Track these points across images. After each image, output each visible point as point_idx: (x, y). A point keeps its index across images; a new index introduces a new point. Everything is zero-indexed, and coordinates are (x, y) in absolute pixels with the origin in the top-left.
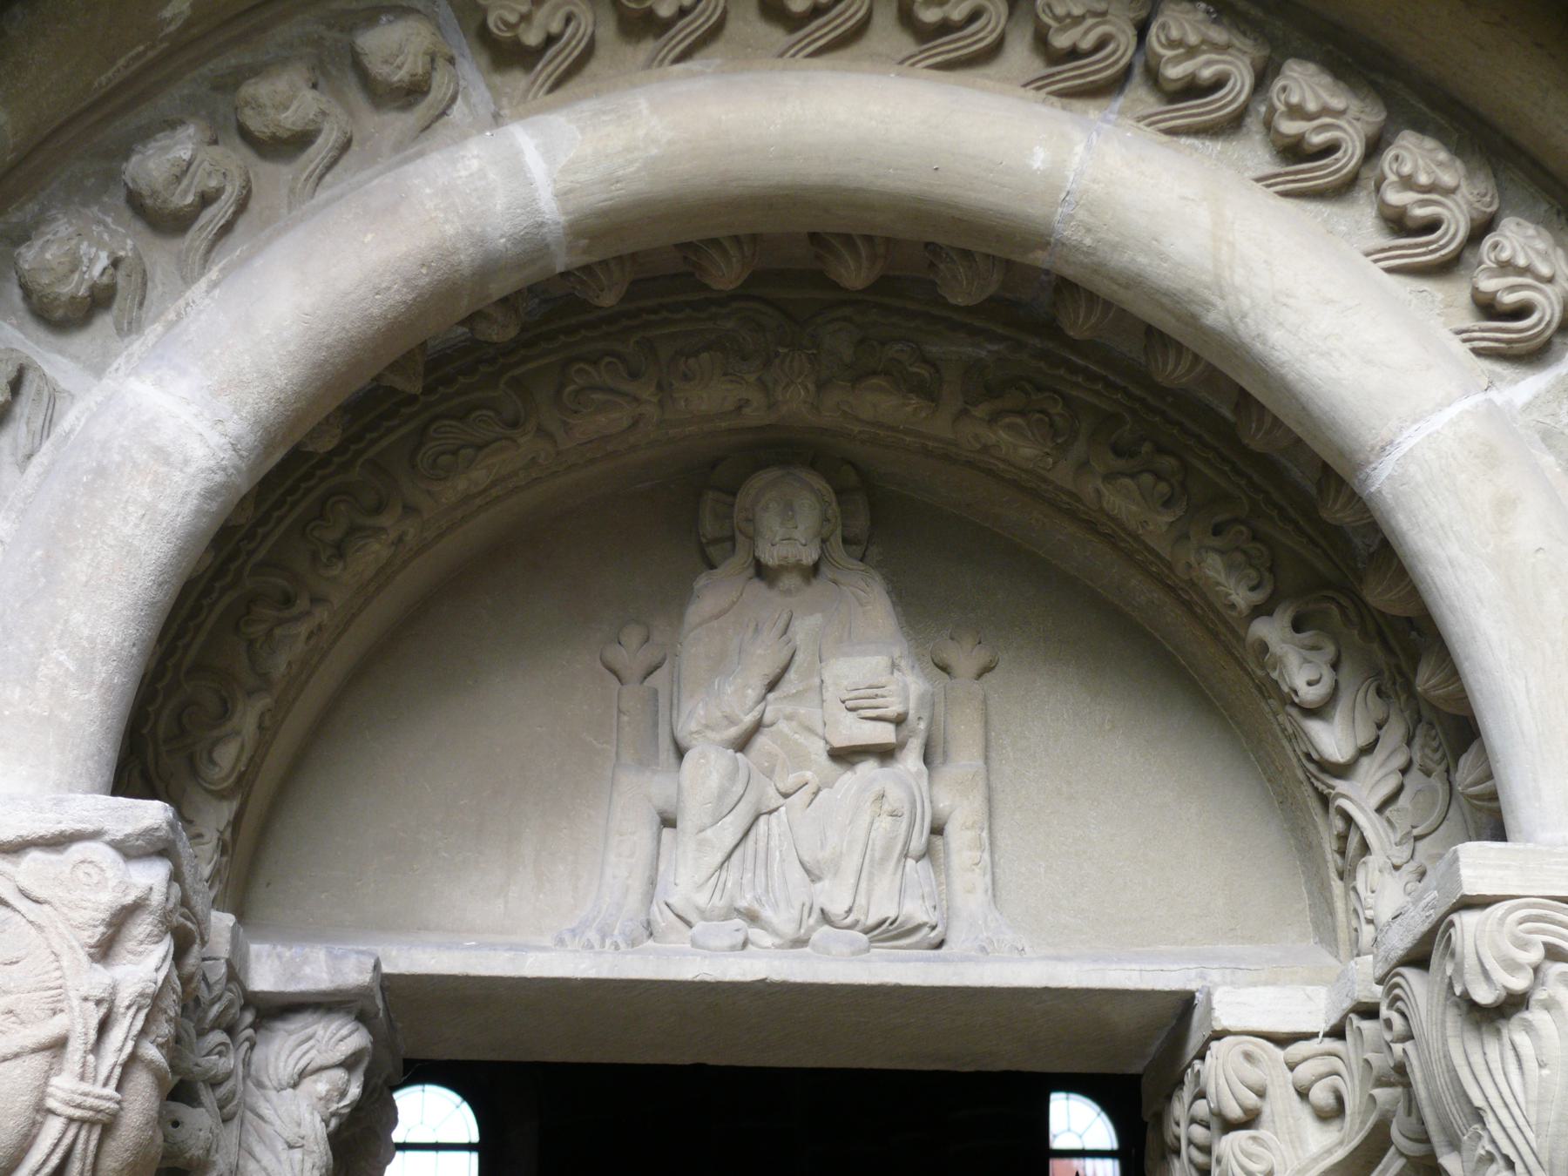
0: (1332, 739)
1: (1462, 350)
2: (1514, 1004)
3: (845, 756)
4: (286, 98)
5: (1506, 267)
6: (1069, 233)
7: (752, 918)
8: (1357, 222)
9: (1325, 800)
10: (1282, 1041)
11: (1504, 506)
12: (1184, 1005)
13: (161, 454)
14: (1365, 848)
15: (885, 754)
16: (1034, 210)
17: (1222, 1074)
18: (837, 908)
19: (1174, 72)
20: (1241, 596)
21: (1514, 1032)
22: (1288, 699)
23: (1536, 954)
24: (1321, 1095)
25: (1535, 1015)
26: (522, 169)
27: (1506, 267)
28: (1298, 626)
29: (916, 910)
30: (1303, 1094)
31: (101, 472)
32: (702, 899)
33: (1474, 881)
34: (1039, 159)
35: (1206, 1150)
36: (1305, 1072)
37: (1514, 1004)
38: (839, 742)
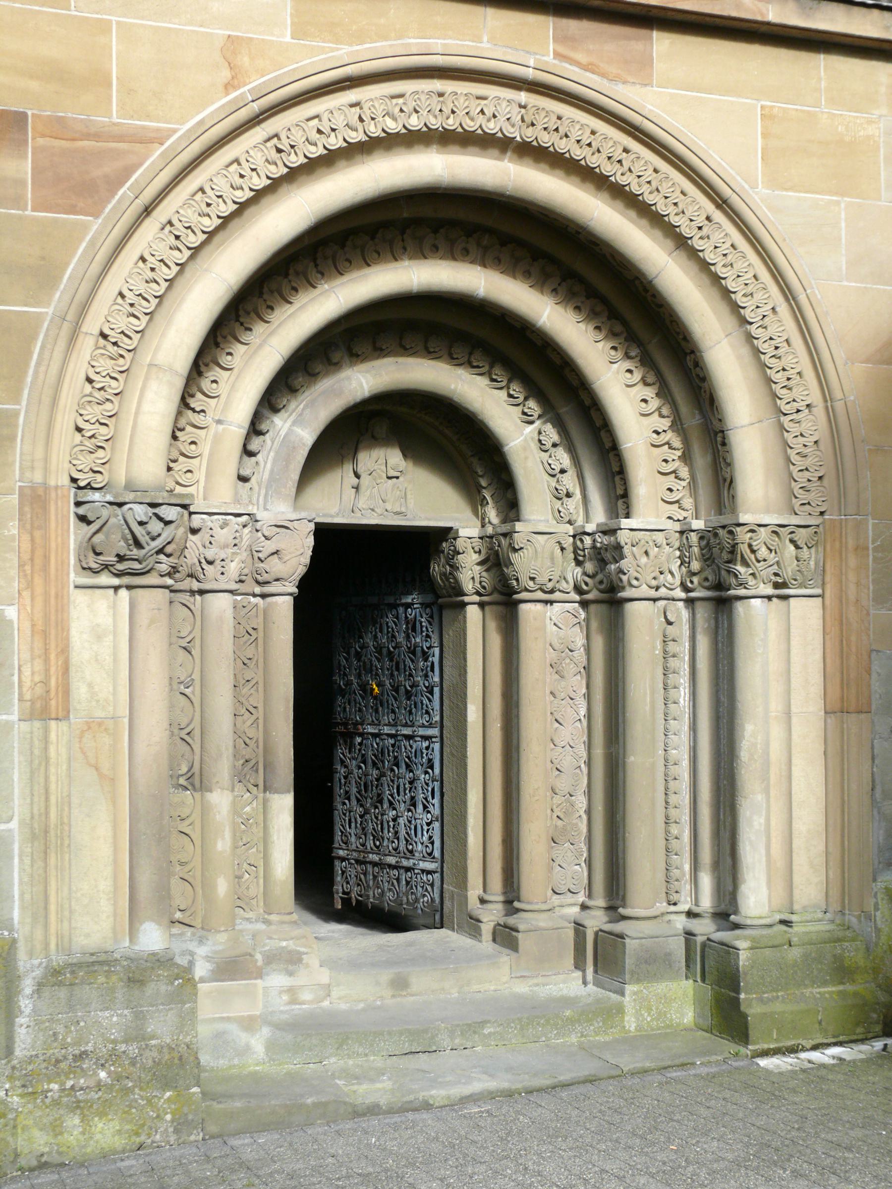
0: (483, 483)
1: (519, 421)
2: (522, 548)
3: (389, 478)
4: (319, 367)
5: (529, 408)
6: (456, 400)
7: (373, 510)
8: (503, 394)
9: (479, 492)
10: (470, 538)
11: (526, 458)
12: (451, 528)
13: (304, 444)
14: (488, 503)
15: (397, 478)
16: (450, 395)
17: (460, 544)
18: (389, 509)
19: (475, 364)
20: (470, 454)
21: (520, 552)
22: (476, 473)
23: (525, 541)
24: (477, 549)
25: (525, 551)
27: (529, 408)
28: (480, 459)
29: (403, 510)
30: (473, 548)
31: (294, 448)
32: (364, 507)
33: (517, 529)
34: (453, 387)
35: (453, 556)
36: (474, 545)
37: (522, 548)
38: (389, 475)
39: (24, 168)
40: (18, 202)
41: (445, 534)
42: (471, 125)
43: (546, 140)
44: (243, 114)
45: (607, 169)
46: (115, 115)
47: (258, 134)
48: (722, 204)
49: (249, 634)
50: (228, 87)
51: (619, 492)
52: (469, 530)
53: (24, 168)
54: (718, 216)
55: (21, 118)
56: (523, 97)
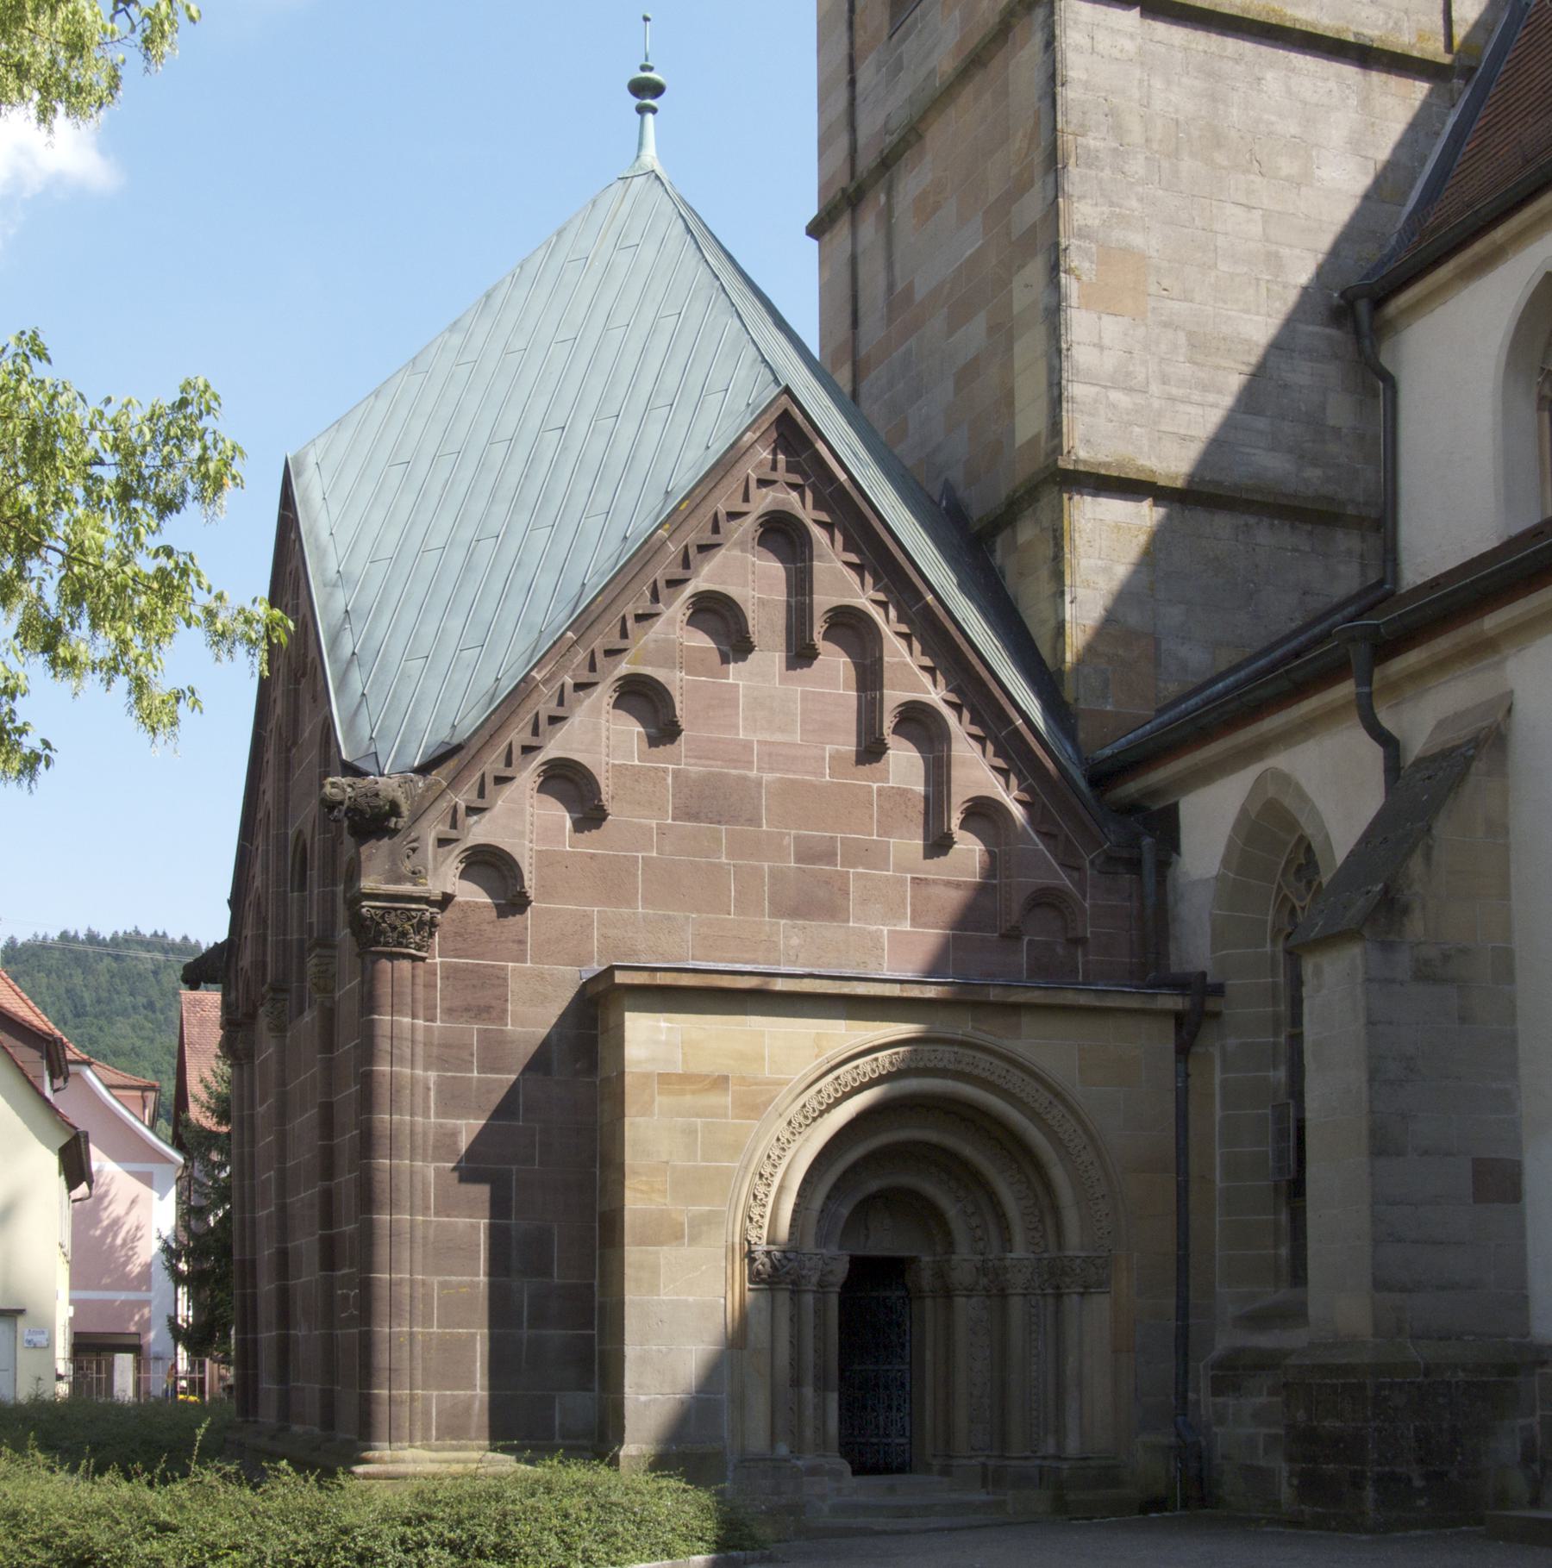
26: (874, 1186)
39: (728, 1100)
40: (726, 1116)
41: (914, 1260)
42: (931, 1065)
43: (968, 1069)
44: (825, 1068)
45: (1000, 1082)
46: (767, 1073)
47: (830, 1077)
48: (1057, 1094)
49: (820, 1313)
50: (817, 1056)
51: (1007, 1242)
52: (926, 1259)
53: (728, 1100)
54: (1055, 1102)
55: (725, 1079)
56: (956, 1049)
